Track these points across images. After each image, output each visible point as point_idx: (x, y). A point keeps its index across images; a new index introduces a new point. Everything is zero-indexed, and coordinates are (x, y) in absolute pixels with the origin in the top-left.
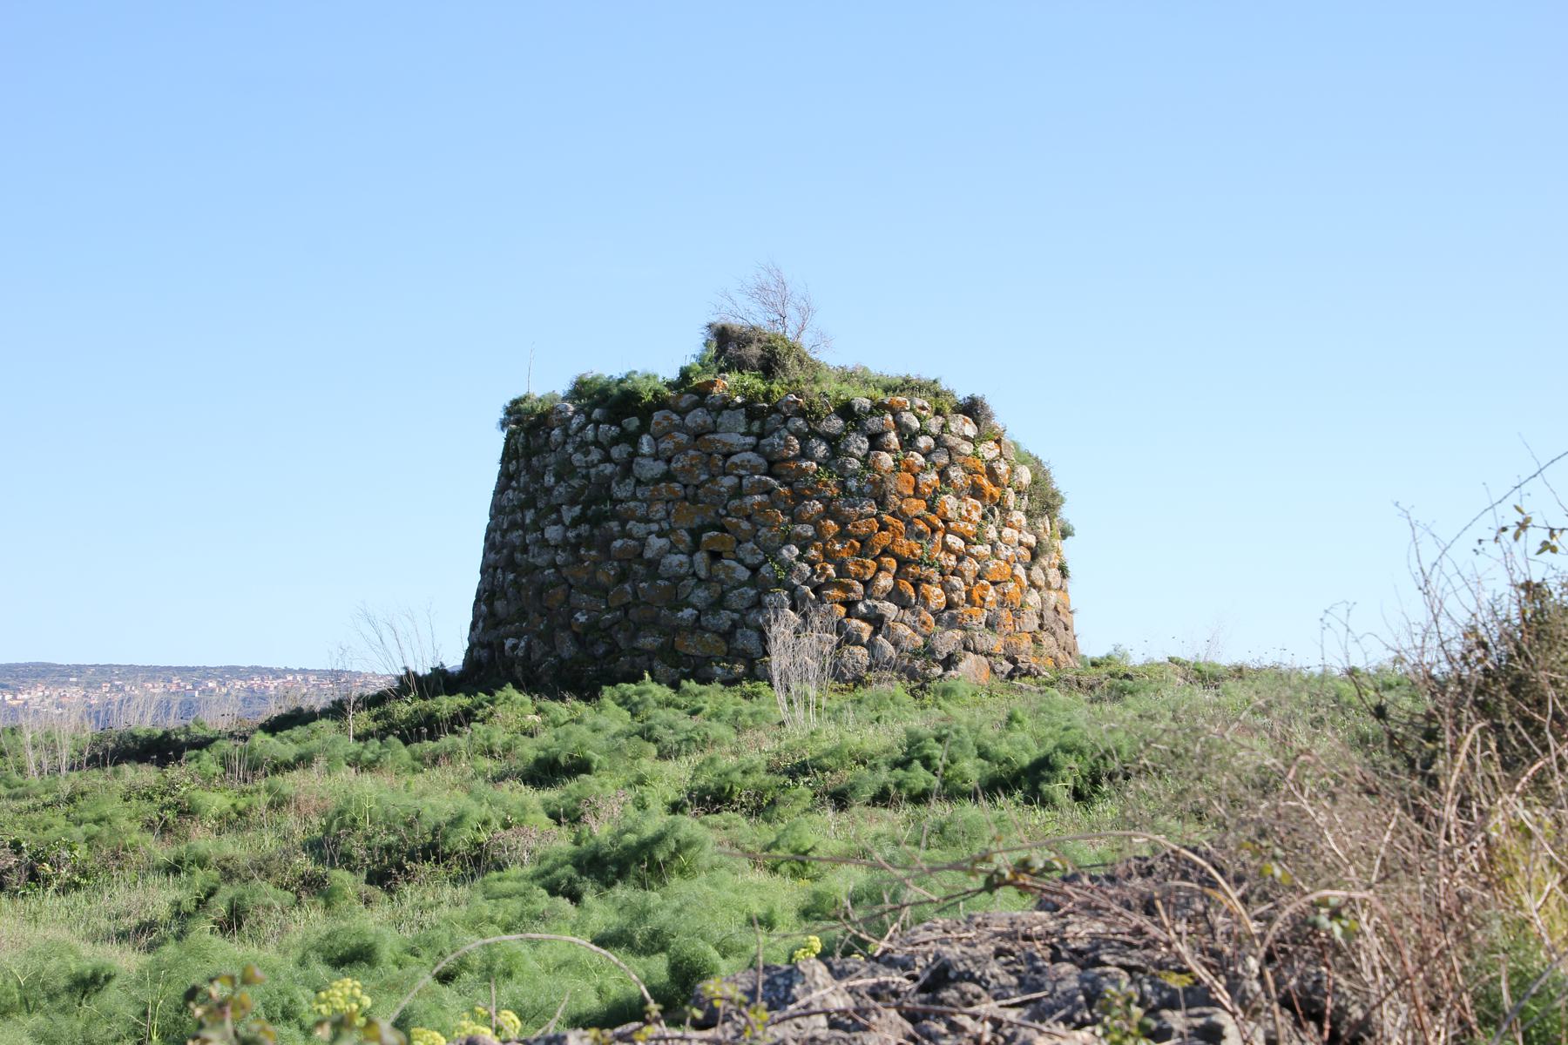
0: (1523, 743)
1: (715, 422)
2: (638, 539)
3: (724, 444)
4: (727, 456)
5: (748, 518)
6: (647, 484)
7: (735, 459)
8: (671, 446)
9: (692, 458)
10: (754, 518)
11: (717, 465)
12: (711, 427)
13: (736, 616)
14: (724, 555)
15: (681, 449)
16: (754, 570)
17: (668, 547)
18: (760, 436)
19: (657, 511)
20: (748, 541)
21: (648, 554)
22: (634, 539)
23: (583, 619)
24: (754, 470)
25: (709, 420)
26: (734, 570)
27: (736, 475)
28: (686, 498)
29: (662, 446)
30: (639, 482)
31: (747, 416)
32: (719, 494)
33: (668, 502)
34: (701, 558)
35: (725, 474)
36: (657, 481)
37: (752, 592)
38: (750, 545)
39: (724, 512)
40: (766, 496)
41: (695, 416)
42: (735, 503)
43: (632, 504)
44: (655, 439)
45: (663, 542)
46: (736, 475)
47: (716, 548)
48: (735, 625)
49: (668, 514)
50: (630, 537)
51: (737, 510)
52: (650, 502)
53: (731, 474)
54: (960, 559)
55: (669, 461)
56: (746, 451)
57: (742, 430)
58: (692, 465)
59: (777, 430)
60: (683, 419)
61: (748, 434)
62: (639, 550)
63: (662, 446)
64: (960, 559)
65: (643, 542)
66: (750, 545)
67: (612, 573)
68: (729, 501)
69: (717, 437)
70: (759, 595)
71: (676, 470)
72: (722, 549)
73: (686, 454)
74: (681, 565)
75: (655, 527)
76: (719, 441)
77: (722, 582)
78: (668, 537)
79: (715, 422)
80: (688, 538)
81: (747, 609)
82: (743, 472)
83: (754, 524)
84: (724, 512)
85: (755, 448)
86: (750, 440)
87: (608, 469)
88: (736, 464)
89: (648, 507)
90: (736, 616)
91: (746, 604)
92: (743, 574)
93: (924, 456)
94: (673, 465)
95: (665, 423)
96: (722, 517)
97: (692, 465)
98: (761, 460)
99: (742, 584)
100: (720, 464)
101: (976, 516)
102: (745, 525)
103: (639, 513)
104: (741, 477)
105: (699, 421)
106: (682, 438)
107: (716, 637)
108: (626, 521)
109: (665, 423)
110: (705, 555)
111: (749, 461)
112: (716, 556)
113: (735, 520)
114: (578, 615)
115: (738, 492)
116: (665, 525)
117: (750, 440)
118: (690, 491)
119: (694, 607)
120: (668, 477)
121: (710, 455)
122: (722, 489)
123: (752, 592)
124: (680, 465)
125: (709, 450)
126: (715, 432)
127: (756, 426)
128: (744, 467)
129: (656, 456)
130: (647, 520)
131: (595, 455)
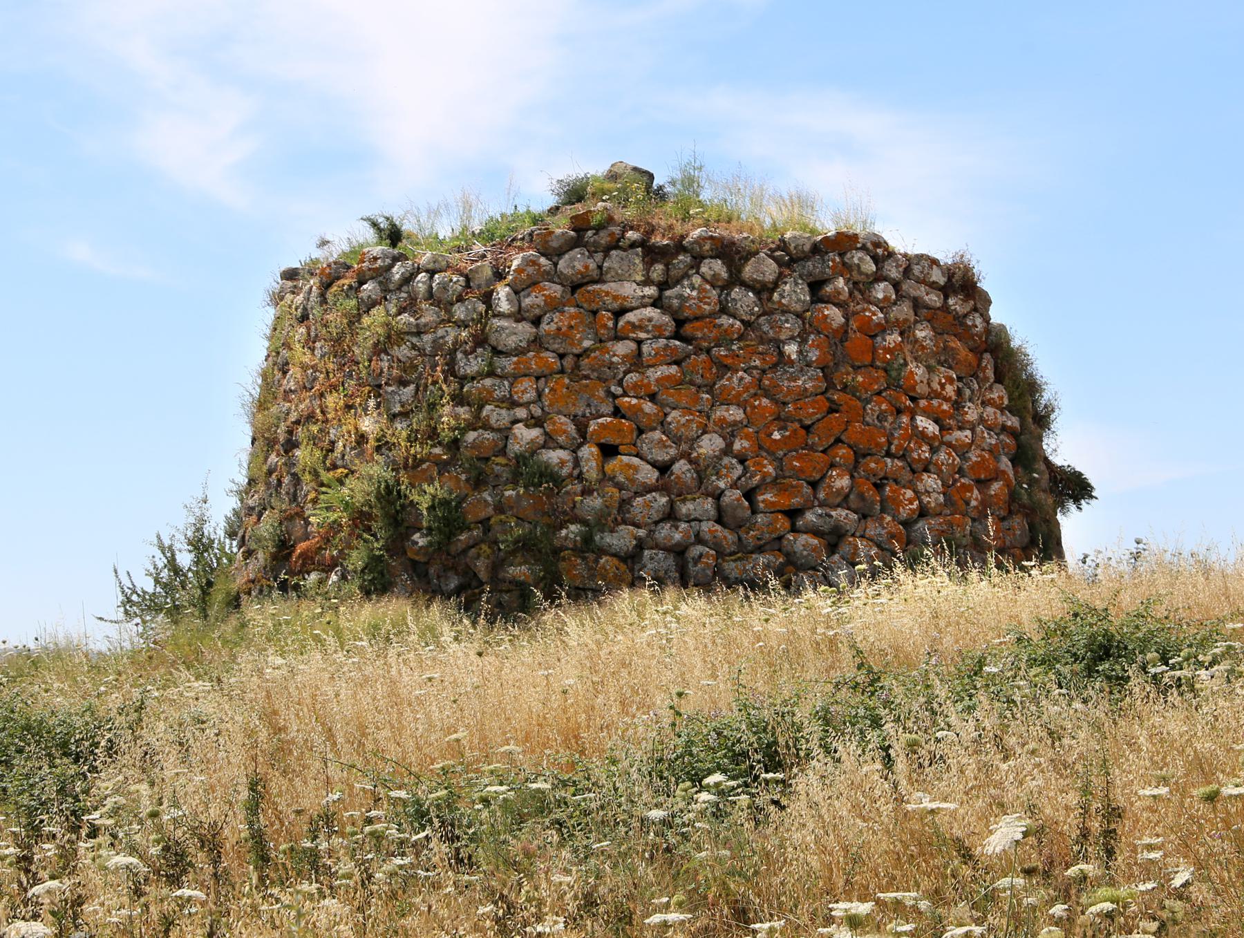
0: (944, 549)
1: (600, 267)
2: (499, 430)
3: (615, 298)
4: (619, 313)
5: (653, 397)
6: (507, 354)
7: (631, 317)
8: (540, 301)
9: (572, 317)
10: (660, 397)
11: (605, 326)
12: (595, 274)
13: (642, 533)
14: (621, 448)
15: (554, 306)
16: (664, 468)
17: (541, 440)
18: (663, 286)
19: (525, 390)
20: (655, 429)
21: (515, 448)
22: (493, 430)
23: (422, 542)
24: (658, 333)
25: (592, 266)
26: (636, 469)
27: (634, 340)
28: (562, 371)
29: (527, 302)
30: (497, 352)
31: (645, 255)
32: (611, 366)
33: (538, 378)
34: (589, 452)
35: (618, 338)
36: (519, 352)
37: (664, 500)
38: (657, 435)
39: (619, 391)
40: (675, 367)
41: (573, 259)
42: (633, 378)
43: (488, 382)
44: (516, 292)
45: (535, 433)
46: (634, 340)
47: (609, 439)
48: (641, 545)
49: (540, 394)
50: (487, 426)
51: (635, 386)
52: (515, 378)
53: (627, 338)
54: (934, 450)
55: (536, 322)
56: (645, 306)
57: (639, 278)
58: (571, 327)
59: (686, 276)
60: (556, 265)
61: (647, 282)
62: (501, 444)
63: (527, 302)
64: (934, 450)
65: (505, 433)
66: (657, 435)
67: (463, 477)
68: (626, 373)
69: (605, 287)
70: (671, 503)
71: (548, 334)
72: (618, 441)
73: (562, 312)
74: (562, 463)
75: (521, 413)
76: (607, 294)
77: (620, 487)
78: (542, 426)
79: (600, 267)
80: (571, 428)
81: (656, 523)
82: (642, 335)
83: (662, 405)
84: (619, 391)
85: (656, 303)
86: (651, 291)
87: (450, 335)
88: (633, 324)
89: (511, 385)
90: (642, 533)
91: (656, 517)
92: (648, 475)
93: (881, 309)
94: (544, 326)
95: (530, 270)
96: (615, 397)
97: (571, 327)
98: (666, 318)
99: (649, 489)
100: (610, 324)
101: (950, 390)
102: (648, 407)
103: (498, 394)
104: (640, 342)
105: (579, 266)
106: (555, 290)
107: (615, 561)
108: (481, 407)
109: (530, 270)
110: (595, 450)
111: (650, 320)
112: (609, 451)
113: (634, 401)
114: (416, 537)
115: (637, 362)
116: (537, 411)
117: (651, 291)
118: (568, 362)
119: (584, 522)
120: (537, 343)
121: (595, 313)
122: (615, 359)
123: (664, 500)
124: (553, 327)
125: (594, 306)
126: (600, 281)
127: (658, 270)
128: (641, 328)
129: (518, 315)
130: (513, 404)
131: (429, 315)
